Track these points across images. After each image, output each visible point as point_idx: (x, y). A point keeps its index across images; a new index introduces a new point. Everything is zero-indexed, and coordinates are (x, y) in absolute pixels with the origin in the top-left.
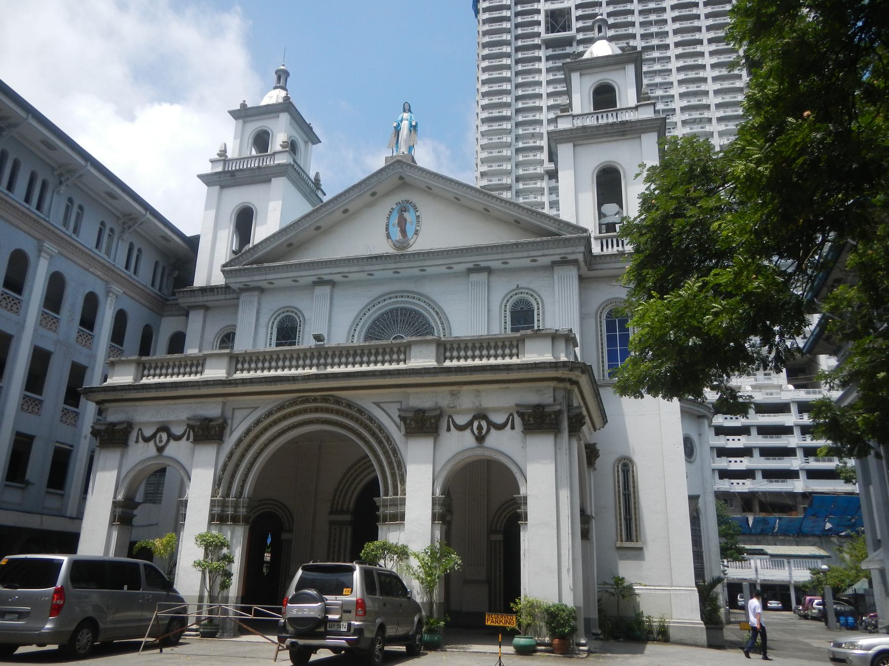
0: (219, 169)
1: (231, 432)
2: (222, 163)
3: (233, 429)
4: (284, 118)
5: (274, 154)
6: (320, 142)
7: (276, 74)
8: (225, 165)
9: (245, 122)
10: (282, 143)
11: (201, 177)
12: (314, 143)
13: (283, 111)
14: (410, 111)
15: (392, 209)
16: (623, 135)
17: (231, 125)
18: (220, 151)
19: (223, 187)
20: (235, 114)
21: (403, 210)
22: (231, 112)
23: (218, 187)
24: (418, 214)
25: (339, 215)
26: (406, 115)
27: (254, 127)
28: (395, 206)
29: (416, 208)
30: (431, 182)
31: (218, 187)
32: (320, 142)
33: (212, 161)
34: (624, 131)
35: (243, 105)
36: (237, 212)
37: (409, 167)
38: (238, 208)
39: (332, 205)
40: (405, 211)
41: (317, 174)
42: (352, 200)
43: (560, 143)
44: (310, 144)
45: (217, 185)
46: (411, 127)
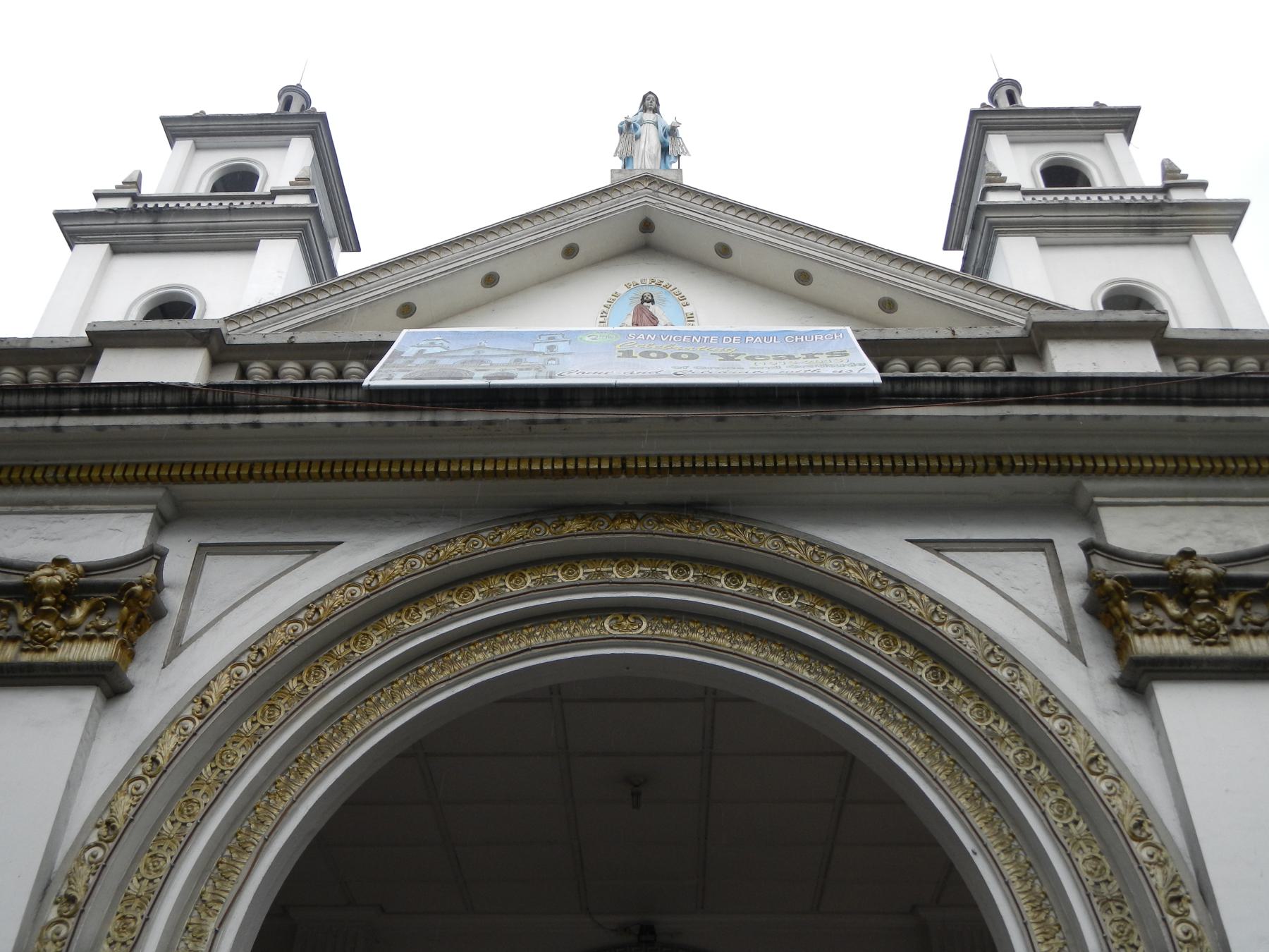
1: (177, 648)
3: (188, 634)
5: (274, 194)
6: (358, 249)
7: (279, 97)
11: (62, 217)
13: (301, 133)
14: (656, 111)
15: (616, 295)
16: (1153, 232)
18: (123, 183)
19: (116, 250)
20: (176, 128)
21: (648, 300)
23: (104, 248)
24: (687, 310)
25: (471, 286)
26: (649, 116)
28: (622, 290)
29: (683, 298)
30: (737, 226)
31: (104, 248)
32: (358, 249)
34: (1153, 223)
36: (147, 304)
37: (676, 194)
39: (457, 251)
40: (652, 301)
42: (521, 249)
43: (1006, 233)
45: (102, 241)
46: (665, 136)
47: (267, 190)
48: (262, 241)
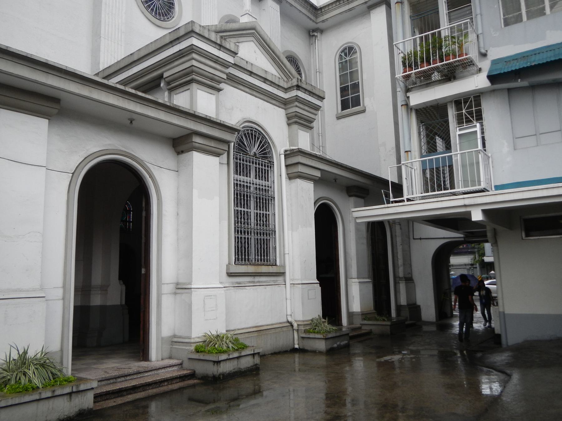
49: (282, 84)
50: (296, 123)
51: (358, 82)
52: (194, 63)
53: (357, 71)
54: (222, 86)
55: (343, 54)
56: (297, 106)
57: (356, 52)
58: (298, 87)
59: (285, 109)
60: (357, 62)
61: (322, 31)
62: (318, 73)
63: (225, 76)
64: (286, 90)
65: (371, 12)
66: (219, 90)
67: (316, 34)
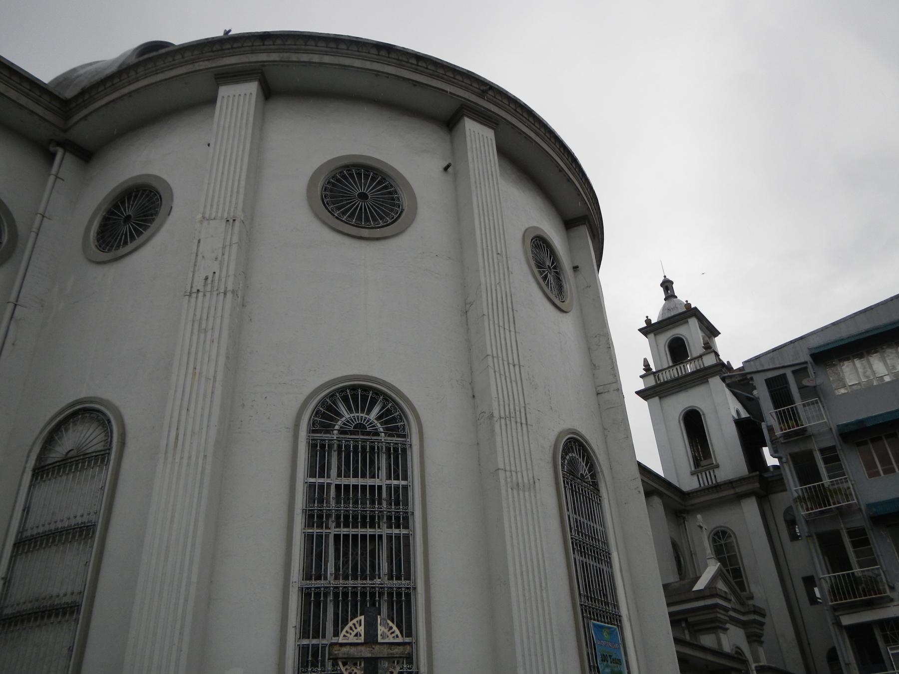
0: (651, 382)
2: (652, 377)
4: (693, 322)
5: (701, 356)
8: (655, 376)
9: (655, 335)
10: (703, 345)
11: (638, 393)
12: (716, 336)
13: (690, 317)
17: (644, 341)
20: (645, 331)
22: (640, 330)
23: (657, 398)
27: (665, 338)
33: (641, 377)
35: (648, 321)
38: (683, 413)
41: (728, 362)
44: (713, 338)
47: (695, 355)
48: (709, 380)
49: (742, 610)
50: (756, 641)
51: (739, 567)
52: (719, 615)
53: (735, 555)
54: (728, 626)
55: (716, 537)
56: (755, 627)
57: (731, 536)
58: (755, 612)
59: (745, 629)
60: (734, 546)
61: (688, 512)
62: (693, 555)
63: (727, 618)
64: (744, 614)
65: (741, 501)
66: (727, 629)
67: (684, 515)
